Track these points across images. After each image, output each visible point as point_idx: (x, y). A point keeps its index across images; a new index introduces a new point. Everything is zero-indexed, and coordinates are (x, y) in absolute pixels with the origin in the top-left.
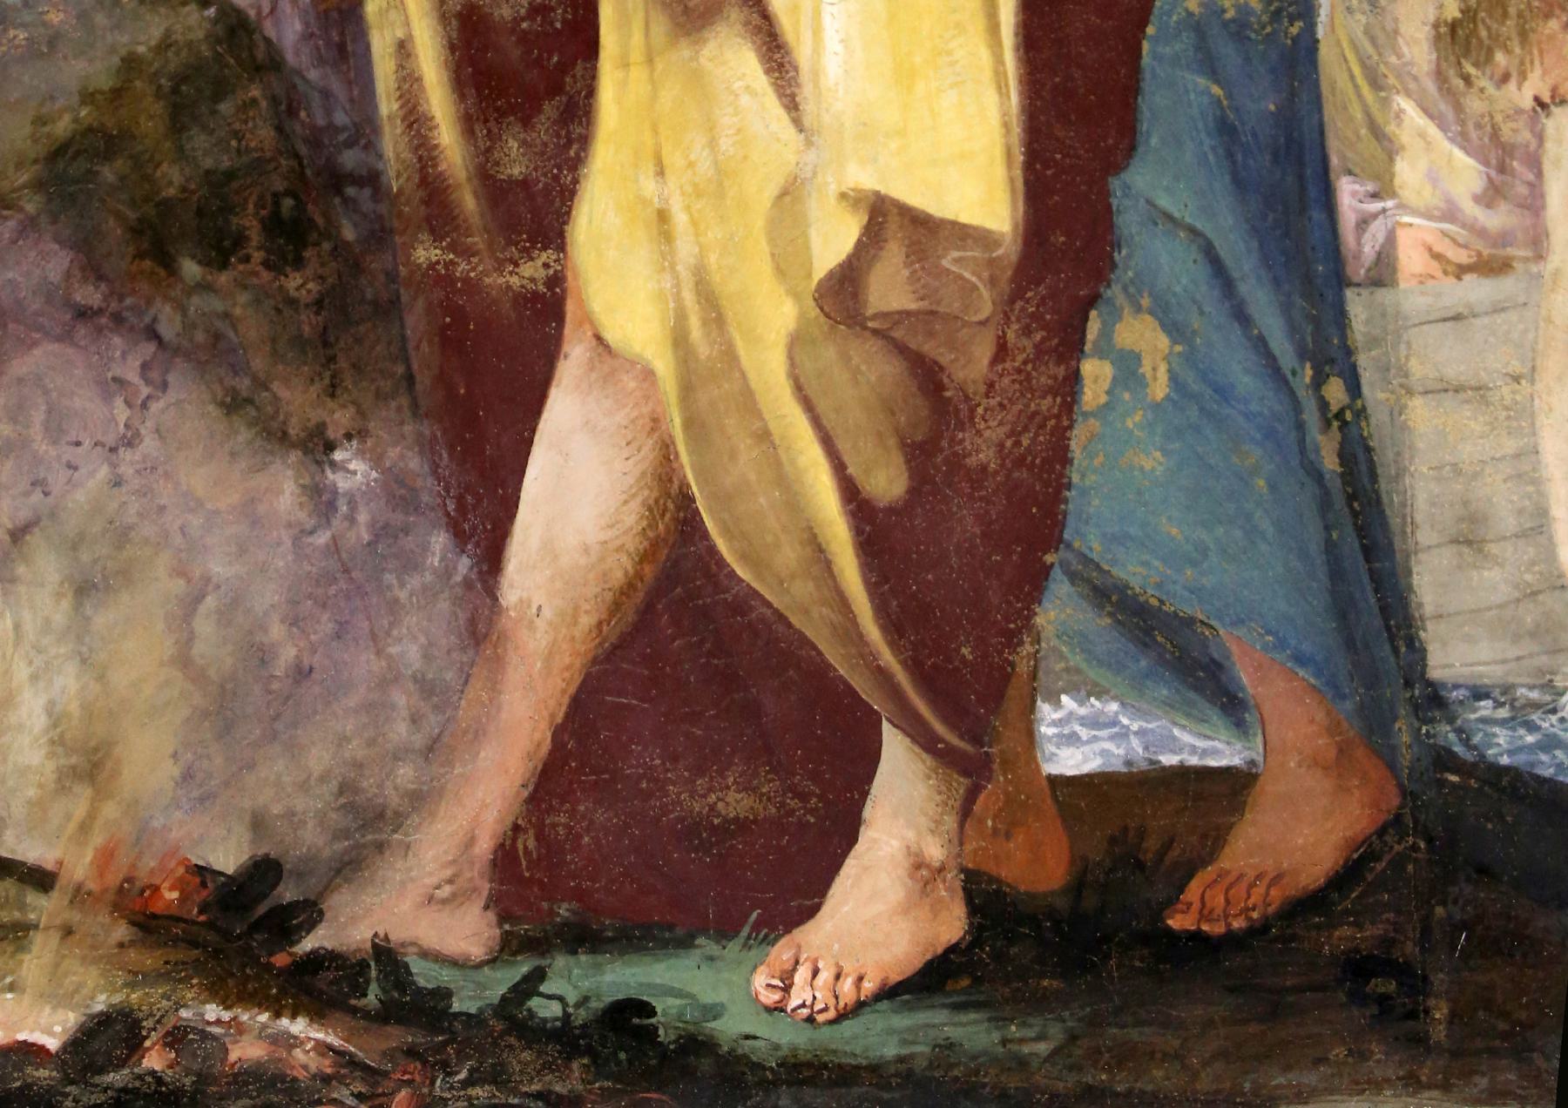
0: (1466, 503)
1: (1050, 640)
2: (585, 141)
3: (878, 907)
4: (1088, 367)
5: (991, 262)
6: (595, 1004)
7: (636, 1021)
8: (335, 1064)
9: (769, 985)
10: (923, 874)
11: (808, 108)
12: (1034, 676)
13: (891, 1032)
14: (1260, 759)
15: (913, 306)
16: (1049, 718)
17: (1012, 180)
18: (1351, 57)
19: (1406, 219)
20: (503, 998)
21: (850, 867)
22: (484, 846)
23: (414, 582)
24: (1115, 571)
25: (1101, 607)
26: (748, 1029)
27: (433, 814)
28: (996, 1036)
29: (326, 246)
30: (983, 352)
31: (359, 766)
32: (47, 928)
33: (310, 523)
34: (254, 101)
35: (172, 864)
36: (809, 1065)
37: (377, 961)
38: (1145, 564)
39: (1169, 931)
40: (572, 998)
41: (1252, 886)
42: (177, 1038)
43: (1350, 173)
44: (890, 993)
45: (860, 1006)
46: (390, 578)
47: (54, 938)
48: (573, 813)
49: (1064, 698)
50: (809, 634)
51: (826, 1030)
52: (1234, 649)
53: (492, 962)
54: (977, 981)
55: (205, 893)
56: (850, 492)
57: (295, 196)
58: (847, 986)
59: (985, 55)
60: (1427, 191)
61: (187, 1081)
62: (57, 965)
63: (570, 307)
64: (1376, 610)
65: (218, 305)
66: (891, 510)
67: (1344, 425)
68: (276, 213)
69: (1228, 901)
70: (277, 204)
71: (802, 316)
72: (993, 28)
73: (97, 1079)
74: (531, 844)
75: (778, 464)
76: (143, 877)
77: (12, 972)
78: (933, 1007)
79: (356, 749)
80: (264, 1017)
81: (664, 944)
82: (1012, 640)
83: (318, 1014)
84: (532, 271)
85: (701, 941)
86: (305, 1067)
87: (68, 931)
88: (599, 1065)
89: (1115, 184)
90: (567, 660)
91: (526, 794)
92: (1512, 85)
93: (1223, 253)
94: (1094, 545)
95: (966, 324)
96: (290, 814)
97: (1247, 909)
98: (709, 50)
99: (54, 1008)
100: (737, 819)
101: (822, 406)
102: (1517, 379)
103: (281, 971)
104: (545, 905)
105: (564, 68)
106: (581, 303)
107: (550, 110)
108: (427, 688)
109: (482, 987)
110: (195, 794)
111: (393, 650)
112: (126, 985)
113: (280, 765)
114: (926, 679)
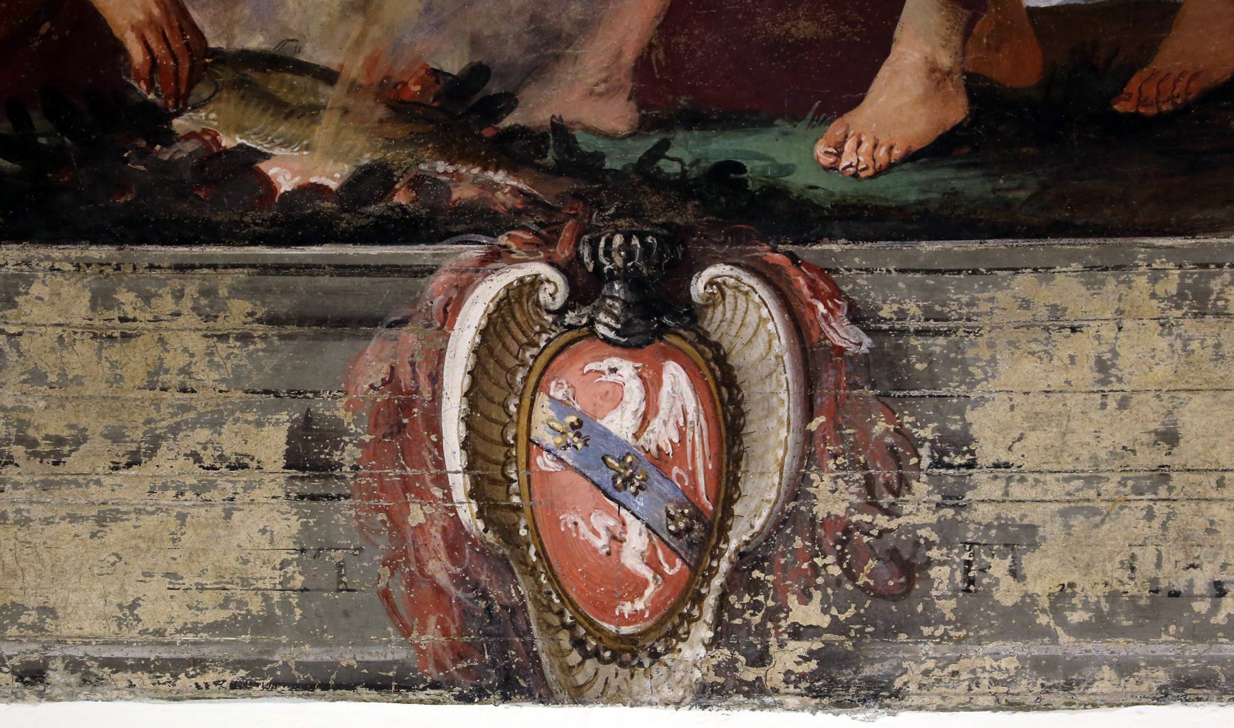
3: (905, 99)
6: (703, 164)
7: (732, 175)
8: (524, 203)
9: (826, 152)
10: (936, 75)
13: (913, 184)
21: (884, 72)
22: (629, 58)
26: (812, 182)
28: (989, 186)
32: (331, 109)
35: (416, 68)
36: (854, 206)
37: (554, 133)
39: (1116, 112)
41: (1177, 81)
42: (417, 183)
44: (911, 157)
45: (890, 167)
47: (336, 116)
51: (867, 183)
53: (632, 135)
55: (438, 87)
58: (882, 152)
61: (423, 212)
62: (338, 134)
69: (1158, 92)
73: (364, 210)
74: (661, 56)
77: (308, 137)
78: (943, 166)
80: (476, 171)
81: (752, 124)
83: (513, 168)
86: (504, 204)
87: (346, 111)
91: (658, 23)
96: (497, 35)
97: (1173, 97)
99: (336, 162)
103: (488, 140)
104: (670, 97)
109: (627, 152)
110: (432, 22)
112: (384, 147)
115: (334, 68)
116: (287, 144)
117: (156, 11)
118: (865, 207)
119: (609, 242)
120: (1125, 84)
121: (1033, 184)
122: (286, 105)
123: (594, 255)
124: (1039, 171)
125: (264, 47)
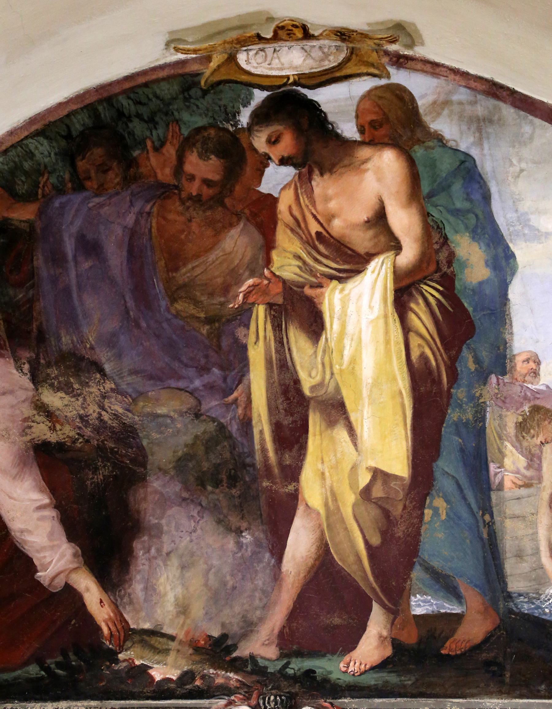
0: (519, 546)
1: (414, 581)
2: (305, 455)
3: (371, 647)
4: (426, 511)
5: (403, 485)
6: (301, 670)
7: (312, 675)
9: (344, 666)
11: (359, 445)
12: (410, 590)
13: (373, 678)
14: (465, 611)
15: (383, 496)
16: (414, 600)
17: (408, 464)
18: (494, 432)
19: (506, 473)
20: (280, 669)
22: (276, 631)
23: (261, 565)
24: (431, 563)
25: (427, 572)
27: (264, 623)
28: (398, 679)
29: (242, 482)
30: (400, 507)
31: (247, 611)
33: (236, 551)
34: (225, 446)
35: (203, 635)
36: (353, 686)
38: (439, 561)
39: (441, 653)
40: (296, 669)
42: (203, 677)
43: (493, 462)
44: (373, 668)
45: (365, 672)
46: (255, 565)
48: (298, 623)
49: (417, 595)
50: (356, 578)
51: (358, 678)
52: (460, 583)
53: (277, 660)
54: (394, 666)
56: (366, 542)
57: (235, 470)
58: (363, 666)
59: (403, 432)
60: (512, 467)
61: (205, 688)
62: (176, 659)
63: (300, 497)
64: (495, 574)
65: (216, 497)
66: (376, 548)
67: (489, 526)
68: (230, 474)
70: (230, 472)
71: (356, 498)
72: (405, 424)
74: (288, 630)
75: (349, 536)
76: (196, 638)
77: (165, 661)
78: (383, 672)
79: (246, 607)
80: (223, 673)
82: (405, 581)
83: (236, 671)
84: (291, 488)
85: (328, 655)
86: (233, 685)
87: (178, 651)
88: (302, 685)
89: (434, 465)
90: (297, 585)
92: (535, 438)
93: (461, 483)
94: (426, 557)
95: (396, 500)
96: (230, 623)
97: (461, 649)
98: (335, 431)
100: (337, 625)
101: (361, 521)
102: (533, 514)
104: (291, 646)
105: (300, 436)
106: (303, 496)
107: (296, 447)
108: (264, 592)
109: (275, 666)
111: (256, 582)
112: (192, 664)
113: (228, 611)
114: (383, 591)
115: (174, 635)
116: (158, 663)
117: (112, 615)
118: (357, 686)
119: (269, 699)
120: (445, 643)
121: (413, 679)
122: (158, 649)
123: (264, 703)
124: (416, 674)
125: (150, 627)
